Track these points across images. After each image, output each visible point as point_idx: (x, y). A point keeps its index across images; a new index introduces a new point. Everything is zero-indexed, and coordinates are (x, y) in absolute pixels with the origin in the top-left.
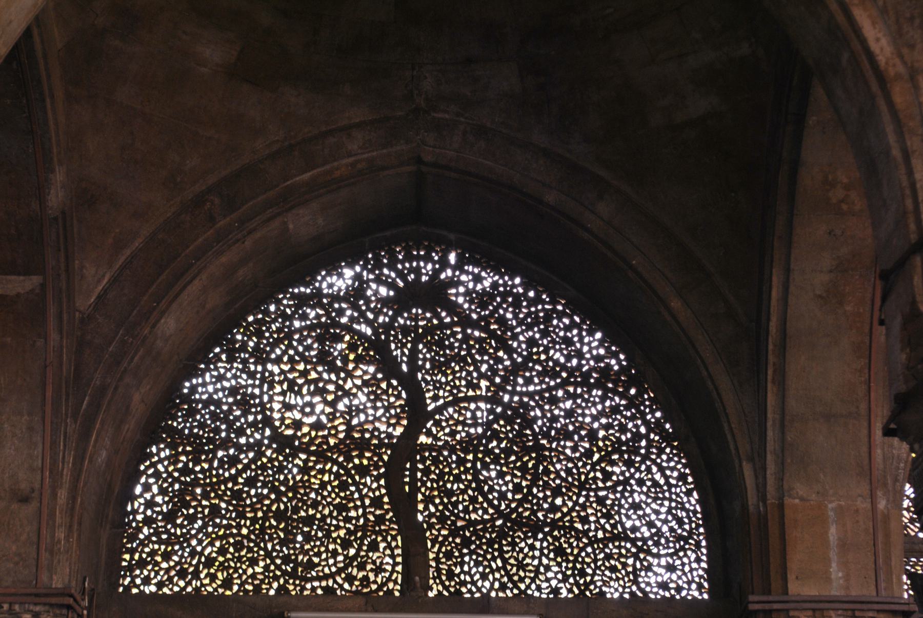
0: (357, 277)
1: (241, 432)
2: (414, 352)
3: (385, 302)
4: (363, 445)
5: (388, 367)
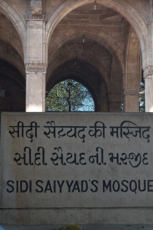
0: (64, 82)
1: (54, 96)
2: (69, 89)
3: (67, 85)
4: (65, 98)
5: (67, 90)
